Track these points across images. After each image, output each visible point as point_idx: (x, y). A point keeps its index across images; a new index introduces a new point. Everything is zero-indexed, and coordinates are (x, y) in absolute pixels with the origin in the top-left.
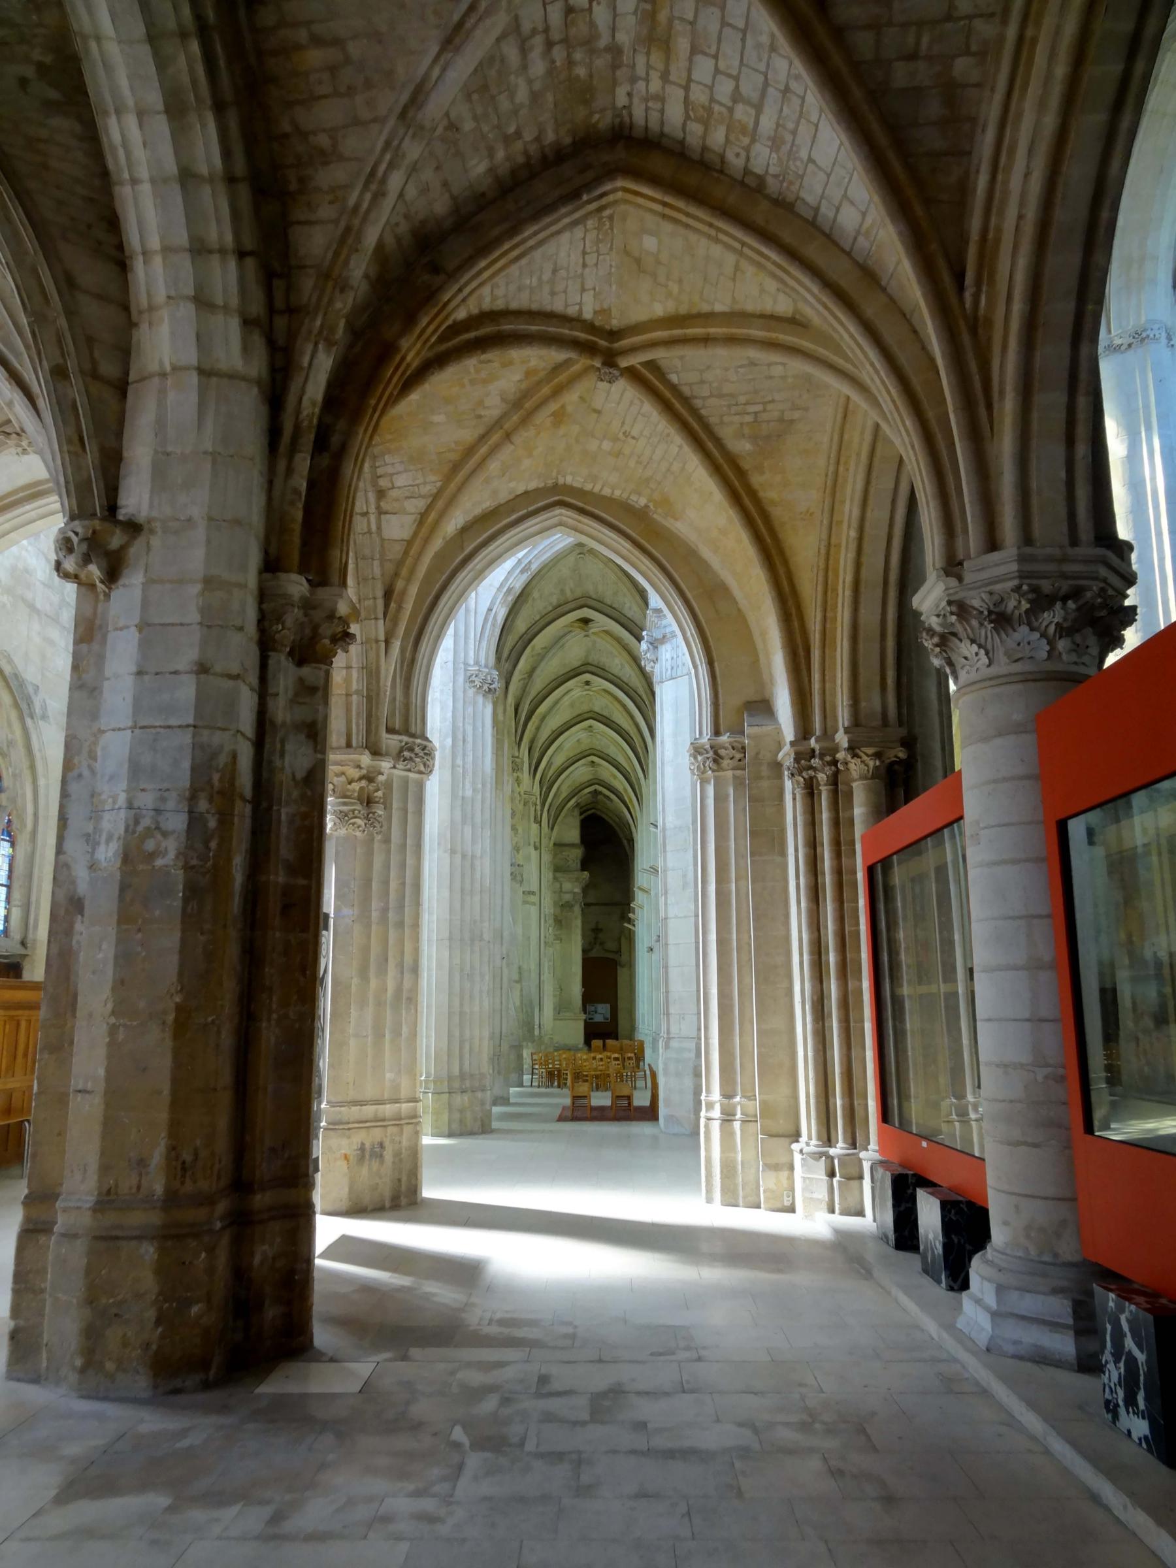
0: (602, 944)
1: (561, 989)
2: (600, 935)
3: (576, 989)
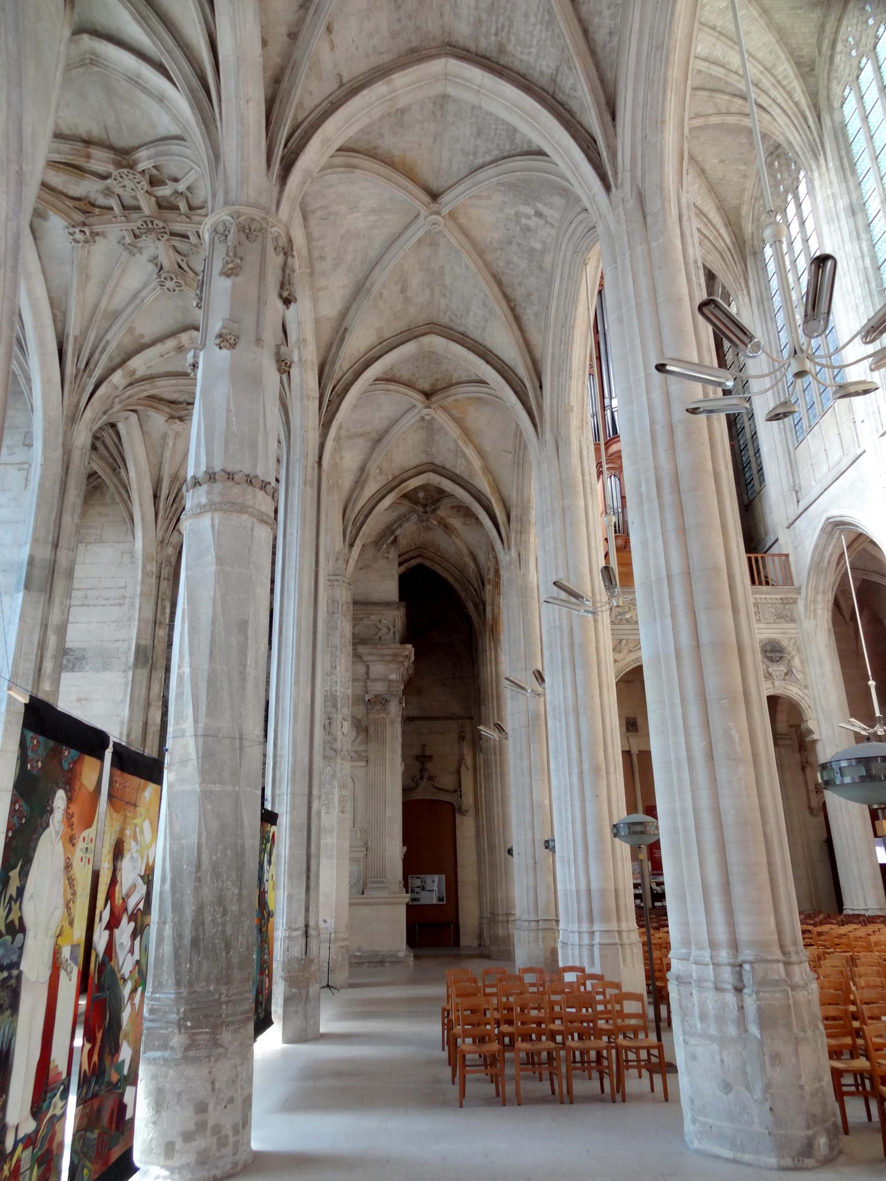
0: (431, 778)
1: (365, 848)
2: (429, 765)
3: (394, 849)
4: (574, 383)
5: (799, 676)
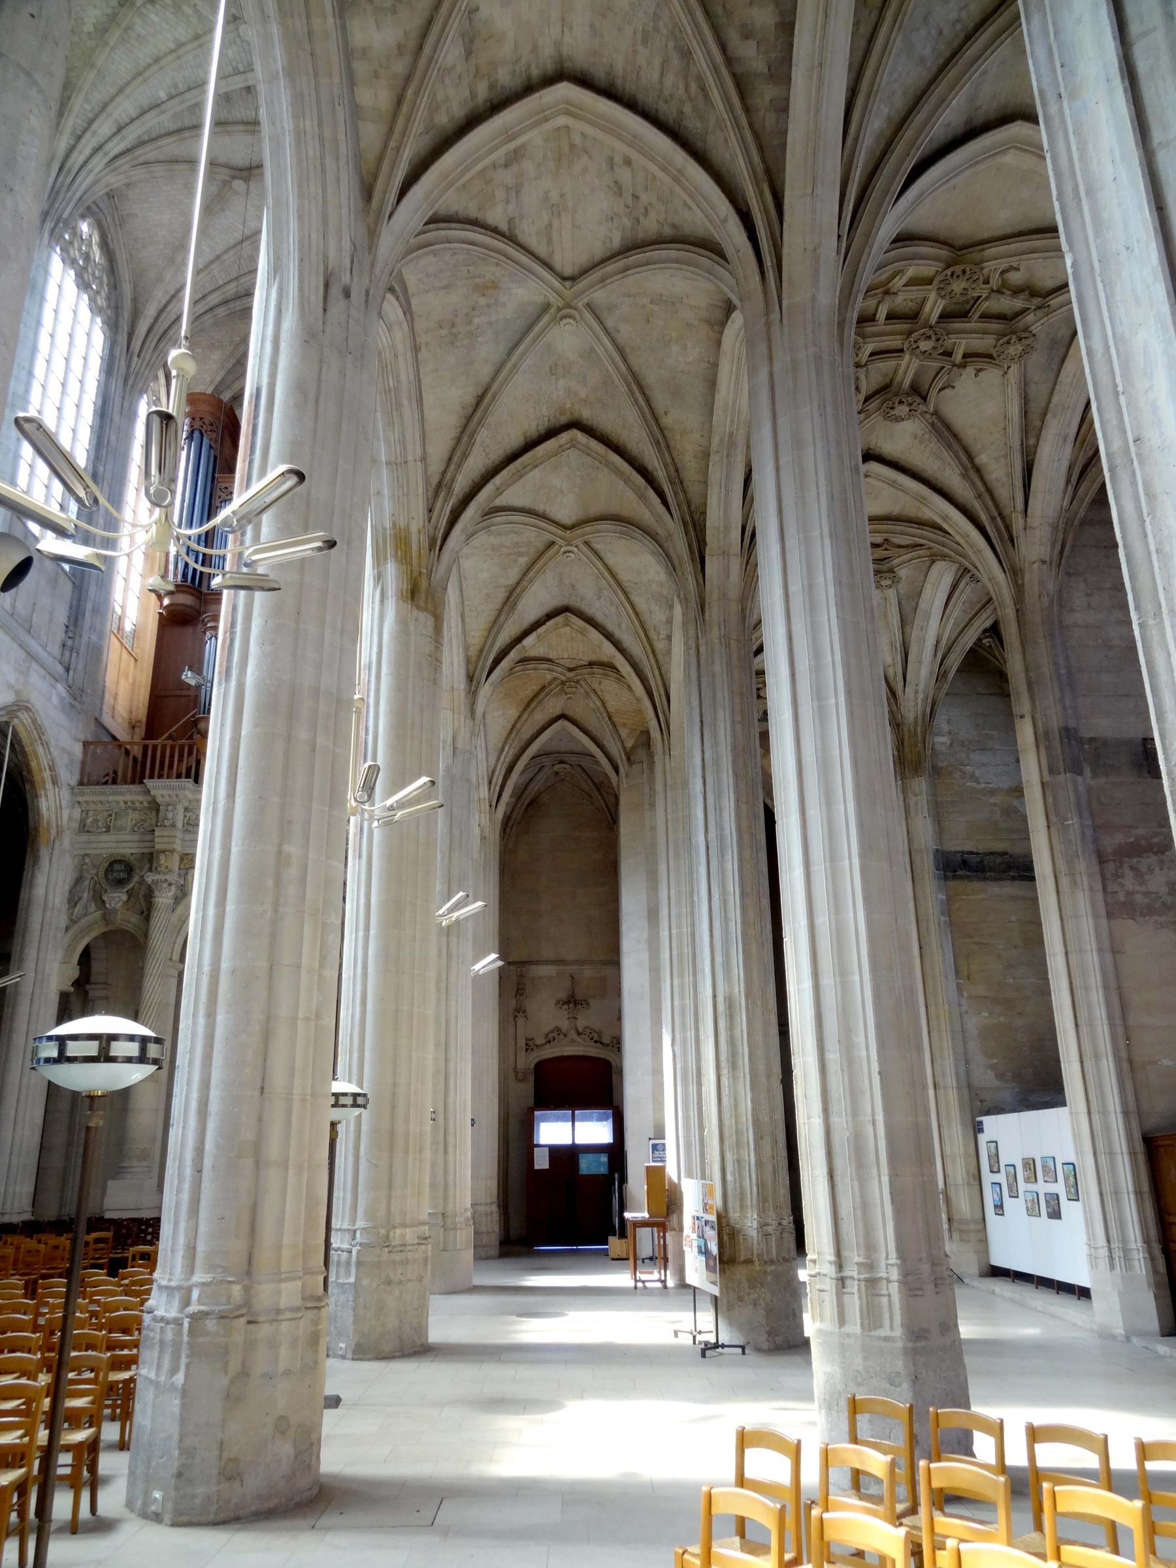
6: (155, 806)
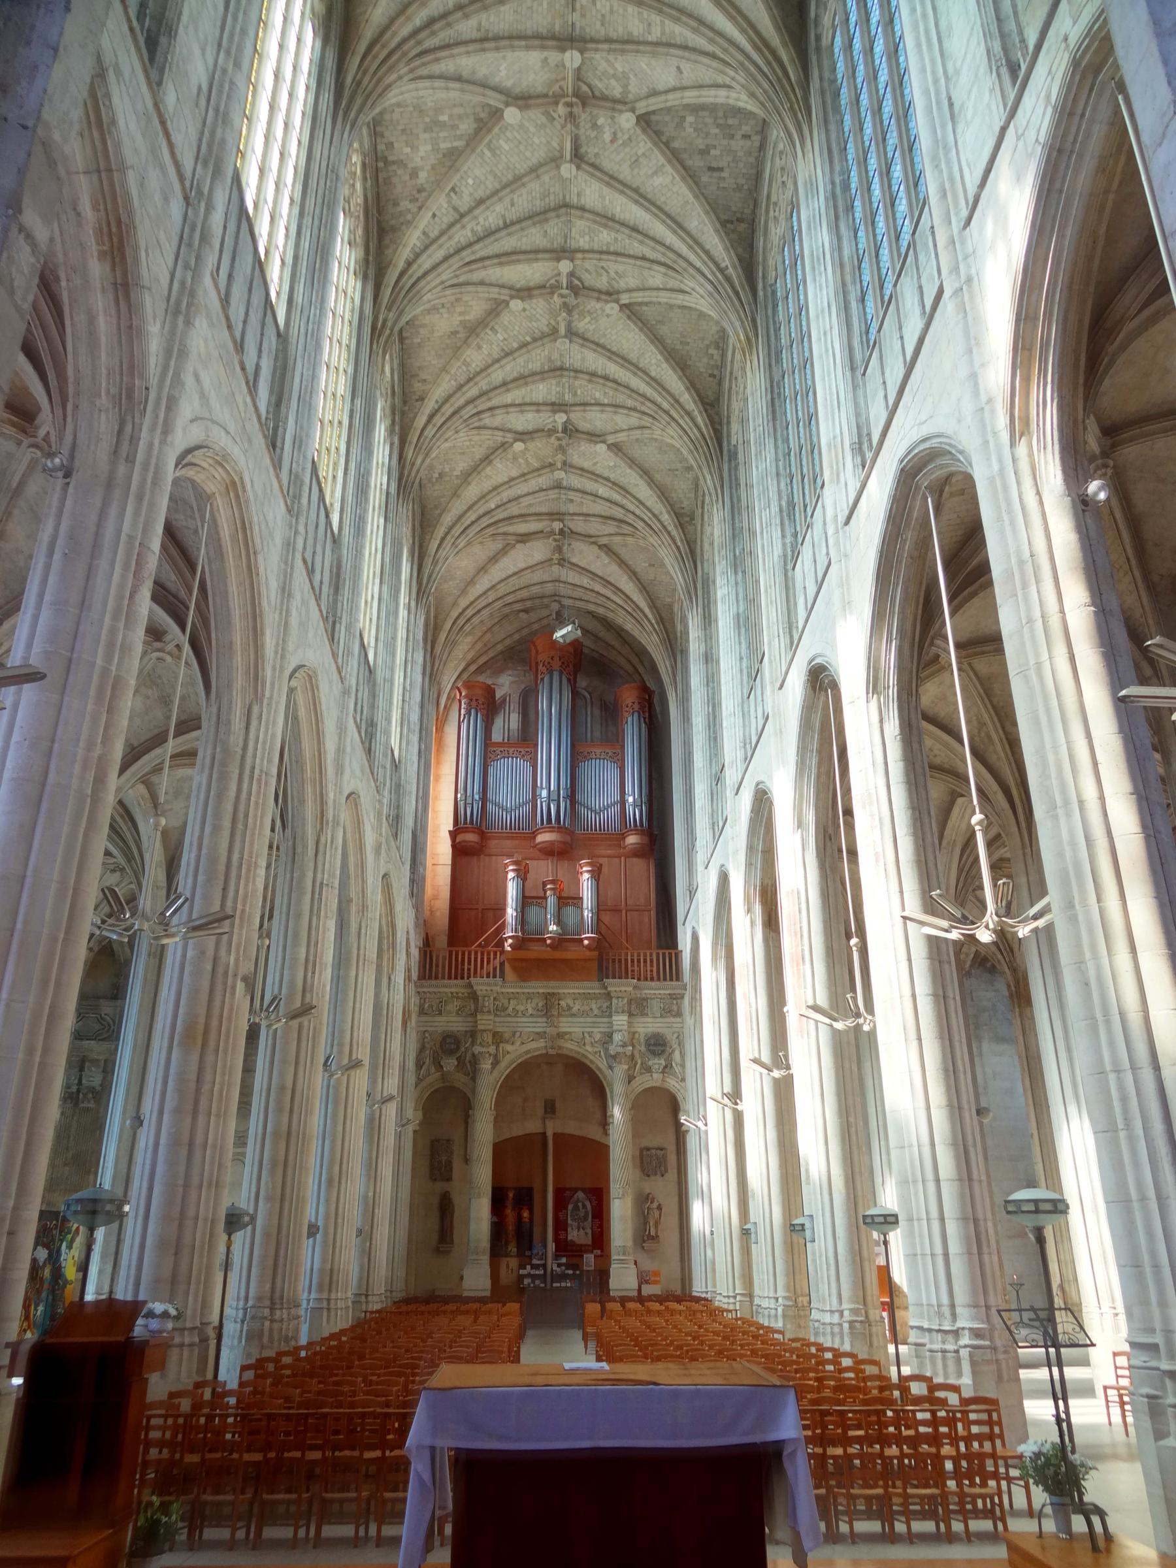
4: (352, 881)
5: (677, 1069)
6: (474, 996)
